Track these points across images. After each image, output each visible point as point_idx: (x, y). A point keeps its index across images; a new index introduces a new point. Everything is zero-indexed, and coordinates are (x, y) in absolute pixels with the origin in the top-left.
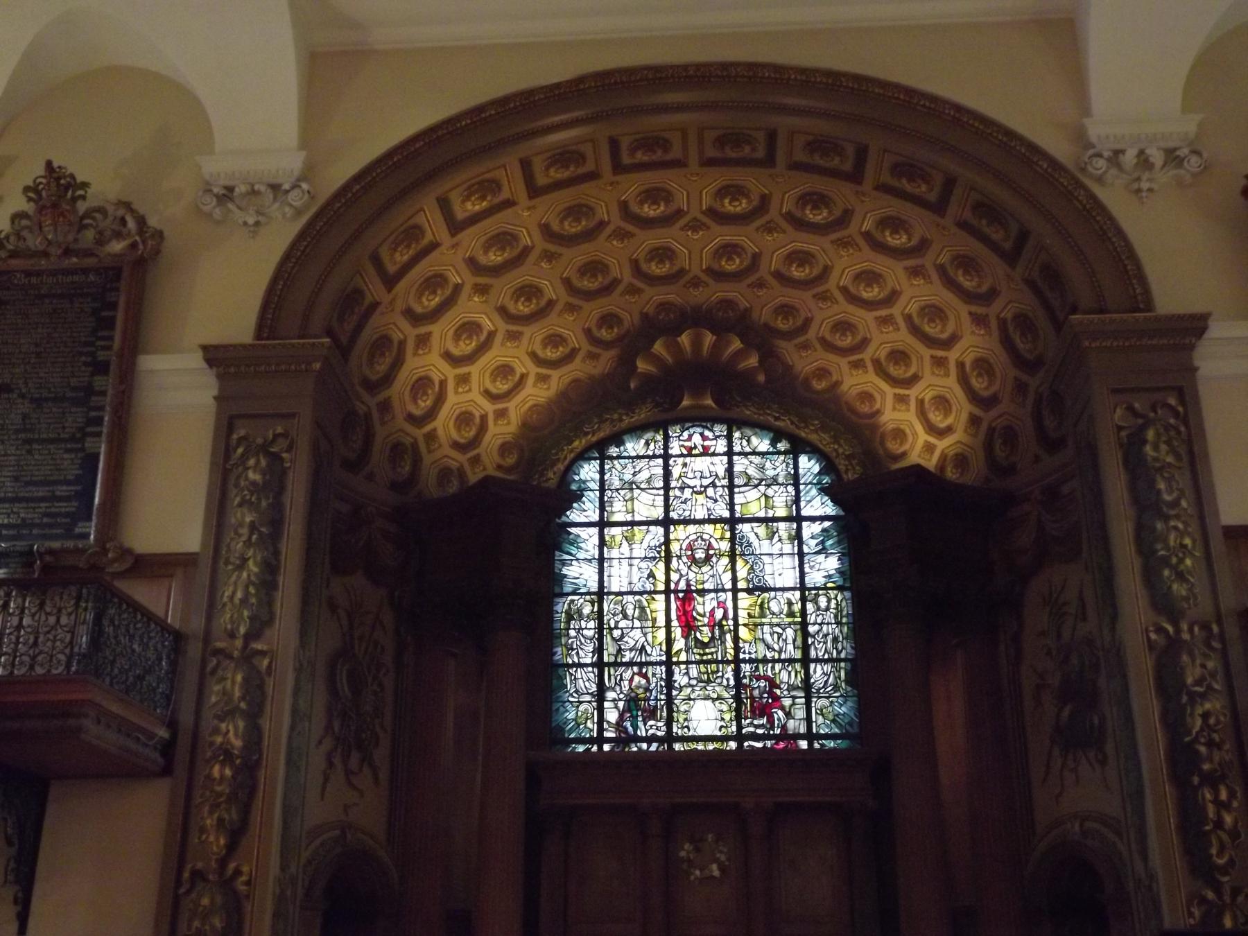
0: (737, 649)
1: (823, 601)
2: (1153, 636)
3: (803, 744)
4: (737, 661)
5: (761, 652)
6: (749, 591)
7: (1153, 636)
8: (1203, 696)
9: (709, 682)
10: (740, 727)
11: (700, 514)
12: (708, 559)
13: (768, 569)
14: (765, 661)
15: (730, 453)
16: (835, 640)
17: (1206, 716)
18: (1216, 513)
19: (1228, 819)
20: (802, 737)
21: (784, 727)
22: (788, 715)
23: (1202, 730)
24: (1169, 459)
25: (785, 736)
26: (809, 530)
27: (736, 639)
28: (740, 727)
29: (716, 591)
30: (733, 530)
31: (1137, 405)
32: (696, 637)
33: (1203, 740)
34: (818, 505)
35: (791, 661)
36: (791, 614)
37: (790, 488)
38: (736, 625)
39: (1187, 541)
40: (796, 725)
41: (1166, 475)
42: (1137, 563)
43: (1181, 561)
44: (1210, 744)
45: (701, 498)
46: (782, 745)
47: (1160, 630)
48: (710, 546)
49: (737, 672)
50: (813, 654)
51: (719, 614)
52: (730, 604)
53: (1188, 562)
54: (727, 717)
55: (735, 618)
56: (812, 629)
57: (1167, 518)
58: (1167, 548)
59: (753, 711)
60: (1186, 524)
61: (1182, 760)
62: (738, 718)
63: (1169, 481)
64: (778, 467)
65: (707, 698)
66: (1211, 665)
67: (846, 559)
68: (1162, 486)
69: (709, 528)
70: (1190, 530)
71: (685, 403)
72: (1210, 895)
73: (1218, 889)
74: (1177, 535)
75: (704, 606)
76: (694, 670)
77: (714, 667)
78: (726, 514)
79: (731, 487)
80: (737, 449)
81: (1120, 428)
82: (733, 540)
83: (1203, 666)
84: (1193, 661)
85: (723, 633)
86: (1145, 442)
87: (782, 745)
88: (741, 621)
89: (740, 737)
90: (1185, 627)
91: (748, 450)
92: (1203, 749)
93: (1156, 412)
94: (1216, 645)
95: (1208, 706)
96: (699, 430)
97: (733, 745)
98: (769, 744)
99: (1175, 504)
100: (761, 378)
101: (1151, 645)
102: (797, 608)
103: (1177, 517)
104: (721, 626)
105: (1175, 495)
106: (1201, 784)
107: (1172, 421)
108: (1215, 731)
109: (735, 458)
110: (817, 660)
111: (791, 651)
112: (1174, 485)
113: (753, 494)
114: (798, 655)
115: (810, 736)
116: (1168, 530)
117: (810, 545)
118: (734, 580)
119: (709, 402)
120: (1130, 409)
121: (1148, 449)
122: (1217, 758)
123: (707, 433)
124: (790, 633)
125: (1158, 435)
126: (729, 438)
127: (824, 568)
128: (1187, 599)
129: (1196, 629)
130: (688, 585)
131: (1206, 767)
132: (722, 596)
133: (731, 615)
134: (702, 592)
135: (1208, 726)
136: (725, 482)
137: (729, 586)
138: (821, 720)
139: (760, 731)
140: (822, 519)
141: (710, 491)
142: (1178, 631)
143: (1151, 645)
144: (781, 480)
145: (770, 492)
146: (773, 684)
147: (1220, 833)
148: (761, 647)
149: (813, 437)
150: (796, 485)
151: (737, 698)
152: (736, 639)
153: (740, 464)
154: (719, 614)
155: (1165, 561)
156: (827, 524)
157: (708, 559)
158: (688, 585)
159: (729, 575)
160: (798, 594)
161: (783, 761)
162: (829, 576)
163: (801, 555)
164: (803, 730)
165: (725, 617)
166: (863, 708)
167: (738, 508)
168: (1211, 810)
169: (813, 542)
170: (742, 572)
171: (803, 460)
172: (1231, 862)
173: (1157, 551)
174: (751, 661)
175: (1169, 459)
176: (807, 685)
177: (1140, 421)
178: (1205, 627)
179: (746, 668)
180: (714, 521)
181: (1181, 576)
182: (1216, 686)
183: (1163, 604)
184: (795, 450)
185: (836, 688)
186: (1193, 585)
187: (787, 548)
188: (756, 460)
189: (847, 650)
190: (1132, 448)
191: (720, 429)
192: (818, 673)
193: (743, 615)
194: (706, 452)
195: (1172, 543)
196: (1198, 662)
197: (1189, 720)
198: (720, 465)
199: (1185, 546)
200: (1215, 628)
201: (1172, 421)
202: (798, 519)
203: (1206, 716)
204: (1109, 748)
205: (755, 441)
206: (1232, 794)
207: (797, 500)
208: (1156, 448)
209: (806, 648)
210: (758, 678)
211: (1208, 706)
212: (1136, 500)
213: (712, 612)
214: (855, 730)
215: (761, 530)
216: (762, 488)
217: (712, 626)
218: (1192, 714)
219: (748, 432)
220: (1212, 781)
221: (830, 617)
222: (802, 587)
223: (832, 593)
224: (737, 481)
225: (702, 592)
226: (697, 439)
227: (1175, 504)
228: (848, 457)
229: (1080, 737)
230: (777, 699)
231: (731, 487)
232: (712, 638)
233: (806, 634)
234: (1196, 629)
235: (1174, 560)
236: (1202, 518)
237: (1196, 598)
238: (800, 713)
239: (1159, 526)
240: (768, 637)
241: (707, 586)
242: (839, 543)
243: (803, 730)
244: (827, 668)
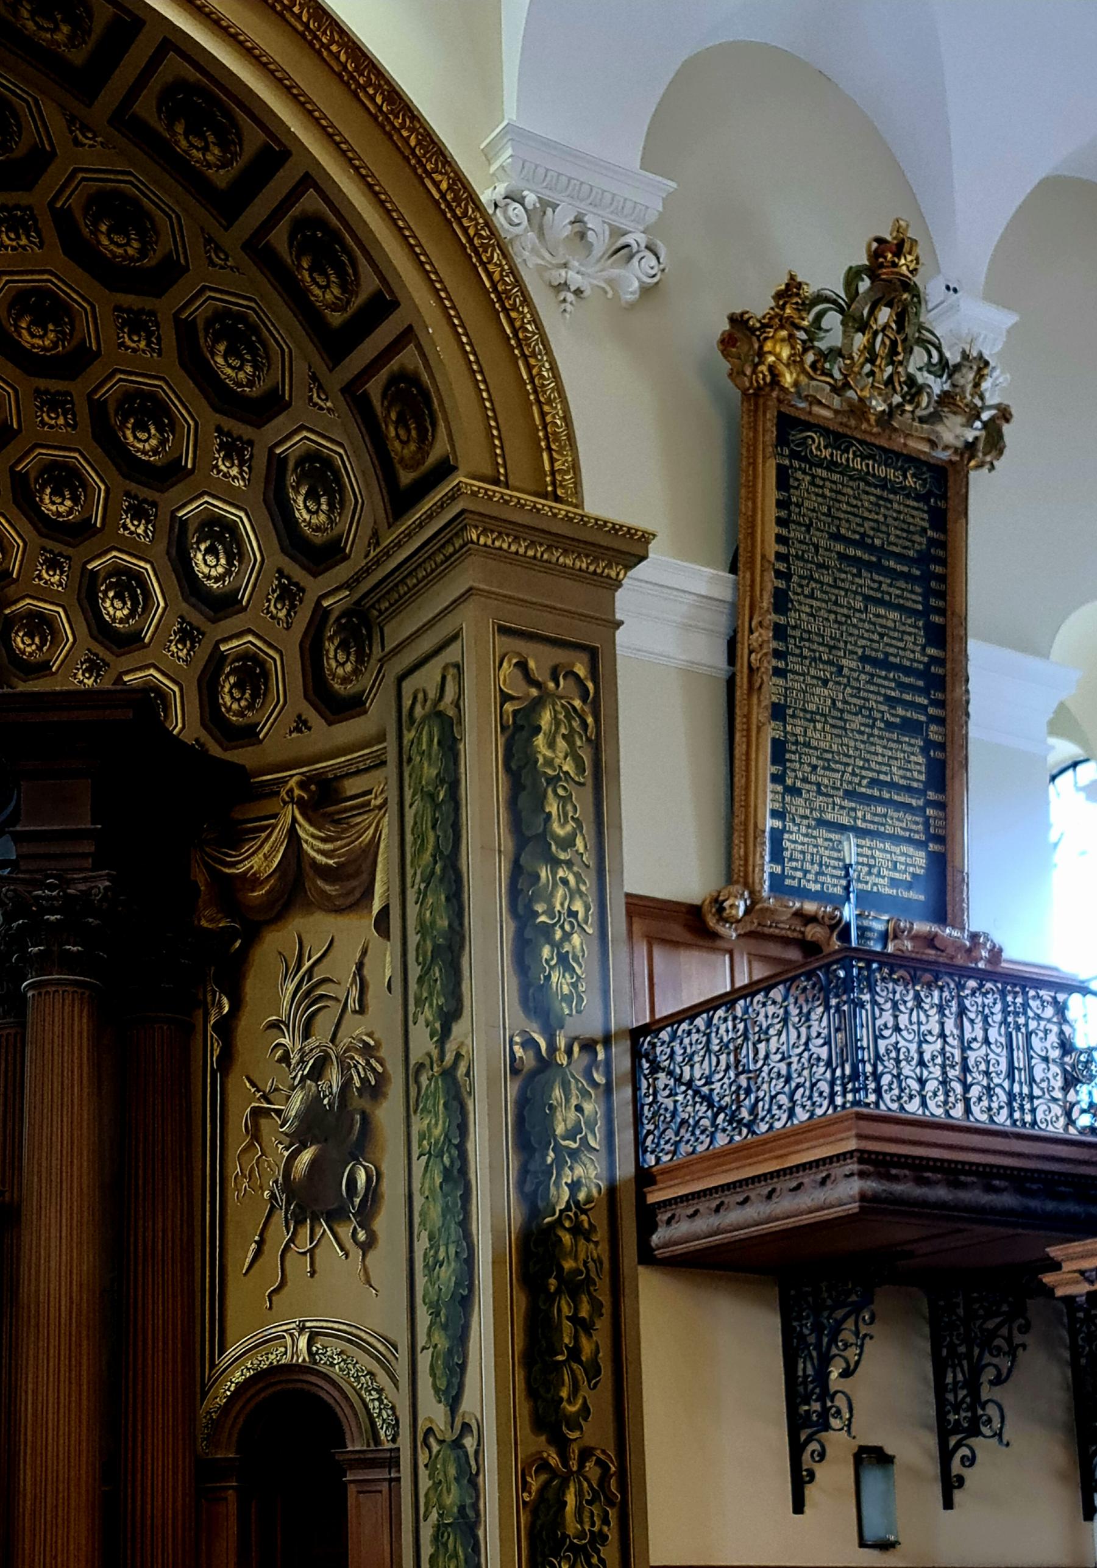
2: (519, 1051)
7: (519, 1051)
8: (574, 1154)
17: (575, 1186)
23: (568, 1207)
24: (568, 767)
31: (532, 664)
33: (567, 1224)
39: (578, 906)
41: (561, 792)
43: (567, 936)
44: (577, 1230)
53: (576, 939)
58: (550, 912)
60: (577, 876)
61: (537, 1251)
63: (564, 800)
66: (588, 1107)
70: (583, 888)
72: (554, 1460)
73: (562, 1445)
83: (579, 1109)
84: (567, 1100)
86: (538, 729)
90: (561, 1042)
92: (567, 1238)
93: (558, 685)
94: (599, 1078)
95: (579, 1171)
99: (568, 843)
103: (569, 864)
105: (569, 828)
106: (558, 1291)
107: (577, 703)
108: (585, 1212)
112: (569, 808)
116: (555, 884)
120: (522, 665)
121: (540, 740)
122: (582, 1256)
125: (557, 723)
128: (568, 999)
129: (576, 1049)
131: (568, 1265)
135: (577, 1203)
142: (552, 1048)
147: (575, 1366)
155: (546, 931)
172: (585, 1410)
173: (536, 914)
175: (568, 767)
177: (534, 692)
182: (593, 1144)
186: (579, 977)
190: (519, 732)
195: (558, 907)
196: (574, 1102)
197: (553, 1189)
199: (573, 914)
200: (601, 1056)
201: (577, 703)
203: (575, 1186)
208: (551, 745)
211: (579, 1171)
218: (557, 1184)
220: (575, 1287)
227: (568, 843)
234: (576, 1049)
235: (558, 934)
237: (580, 999)
239: (544, 873)
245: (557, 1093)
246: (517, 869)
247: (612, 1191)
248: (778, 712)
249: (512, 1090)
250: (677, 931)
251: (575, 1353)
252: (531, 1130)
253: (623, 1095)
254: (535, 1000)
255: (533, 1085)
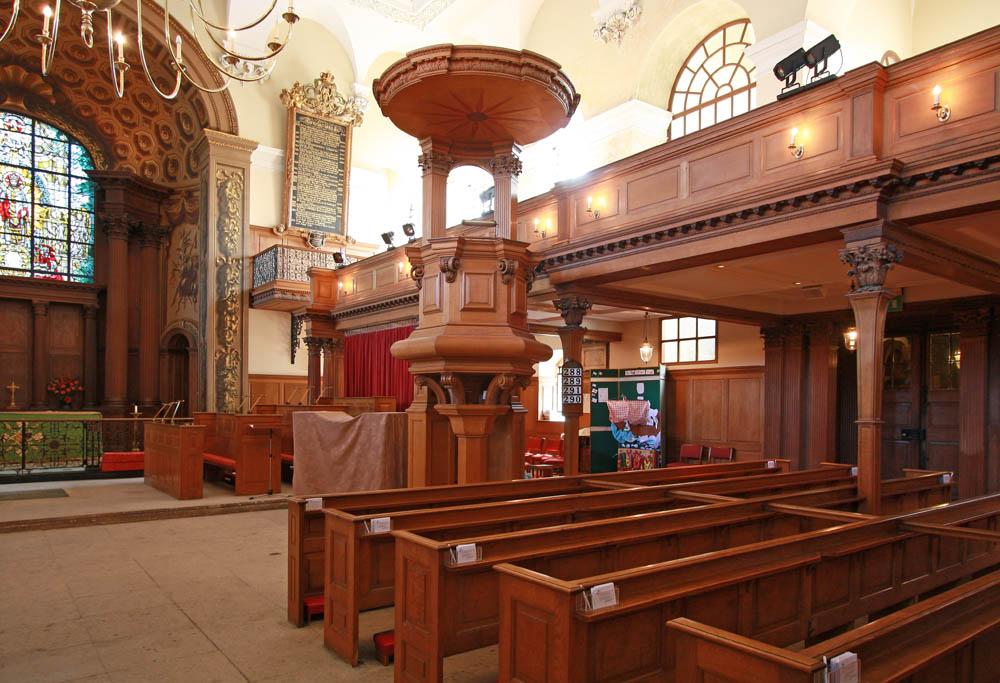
0: (33, 231)
1: (79, 216)
3: (65, 278)
4: (32, 237)
5: (46, 234)
6: (41, 205)
9: (16, 244)
10: (32, 266)
11: (16, 163)
12: (18, 185)
13: (51, 197)
14: (47, 239)
15: (33, 135)
16: (84, 234)
17: (232, 292)
18: (248, 220)
19: (234, 327)
20: (65, 274)
21: (56, 269)
22: (58, 264)
25: (56, 273)
26: (74, 181)
27: (33, 226)
28: (32, 266)
29: (23, 202)
30: (33, 174)
32: (10, 223)
34: (78, 170)
35: (61, 241)
36: (63, 219)
37: (67, 161)
38: (33, 220)
40: (62, 269)
42: (216, 233)
45: (15, 154)
46: (54, 277)
47: (221, 259)
48: (20, 179)
49: (32, 241)
50: (72, 239)
51: (24, 213)
52: (30, 210)
54: (26, 261)
55: (33, 217)
56: (73, 228)
57: (230, 218)
59: (40, 260)
61: (221, 305)
62: (32, 262)
64: (61, 147)
65: (15, 251)
67: (93, 200)
68: (230, 205)
69: (19, 170)
71: (8, 102)
74: (232, 225)
75: (15, 208)
76: (8, 237)
77: (20, 237)
78: (30, 166)
79: (33, 152)
80: (37, 133)
81: (218, 179)
82: (33, 179)
85: (25, 222)
87: (54, 277)
88: (35, 218)
89: (32, 271)
91: (43, 135)
96: (16, 118)
97: (28, 275)
98: (47, 275)
100: (54, 102)
101: (217, 265)
102: (66, 217)
104: (24, 219)
109: (36, 138)
110: (74, 242)
111: (61, 236)
113: (44, 158)
114: (66, 238)
115: (69, 275)
117: (74, 189)
118: (33, 198)
119: (22, 105)
123: (20, 121)
124: (61, 228)
126: (33, 126)
127: (82, 200)
130: (6, 196)
132: (26, 205)
133: (30, 214)
134: (14, 201)
136: (30, 149)
137: (30, 200)
138: (74, 268)
139: (43, 269)
140: (82, 178)
141: (21, 151)
143: (217, 265)
144: (61, 154)
145: (54, 159)
146: (51, 249)
148: (46, 231)
149: (79, 137)
150: (69, 159)
151: (32, 254)
152: (33, 226)
153: (38, 141)
154: (24, 213)
155: (227, 234)
156: (84, 181)
157: (18, 185)
158: (6, 196)
159: (30, 195)
160: (67, 211)
161: (54, 284)
162: (84, 205)
163: (70, 192)
164: (66, 271)
165: (27, 215)
166: (96, 267)
167: (36, 164)
168: (229, 323)
169: (76, 189)
170: (37, 195)
171: (74, 147)
174: (40, 237)
176: (69, 253)
178: (237, 260)
179: (37, 241)
180: (23, 168)
181: (232, 240)
183: (223, 250)
184: (71, 140)
185: (83, 256)
187: (62, 188)
188: (49, 142)
189: (90, 240)
191: (28, 121)
192: (74, 248)
193: (36, 217)
194: (19, 131)
198: (28, 139)
202: (70, 176)
203: (232, 292)
204: (198, 296)
205: (47, 130)
206: (237, 318)
207: (69, 167)
209: (69, 236)
210: (44, 246)
212: (220, 209)
213: (20, 213)
214: (92, 274)
215: (49, 177)
216: (50, 157)
217: (20, 219)
219: (44, 126)
220: (230, 314)
221: (82, 224)
222: (69, 208)
223: (85, 214)
224: (36, 150)
225: (14, 201)
226: (13, 123)
228: (97, 152)
229: (187, 291)
230: (53, 256)
231: (33, 152)
232: (19, 224)
233: (69, 230)
236: (243, 220)
238: (64, 264)
239: (227, 220)
240: (50, 228)
241: (17, 199)
242: (90, 191)
243: (66, 271)
244: (80, 246)
245: (228, 270)
246: (219, 219)
247: (242, 292)
248: (295, 184)
249: (216, 269)
250: (269, 234)
251: (230, 328)
252: (221, 278)
253: (247, 272)
254: (223, 250)
255: (222, 269)
